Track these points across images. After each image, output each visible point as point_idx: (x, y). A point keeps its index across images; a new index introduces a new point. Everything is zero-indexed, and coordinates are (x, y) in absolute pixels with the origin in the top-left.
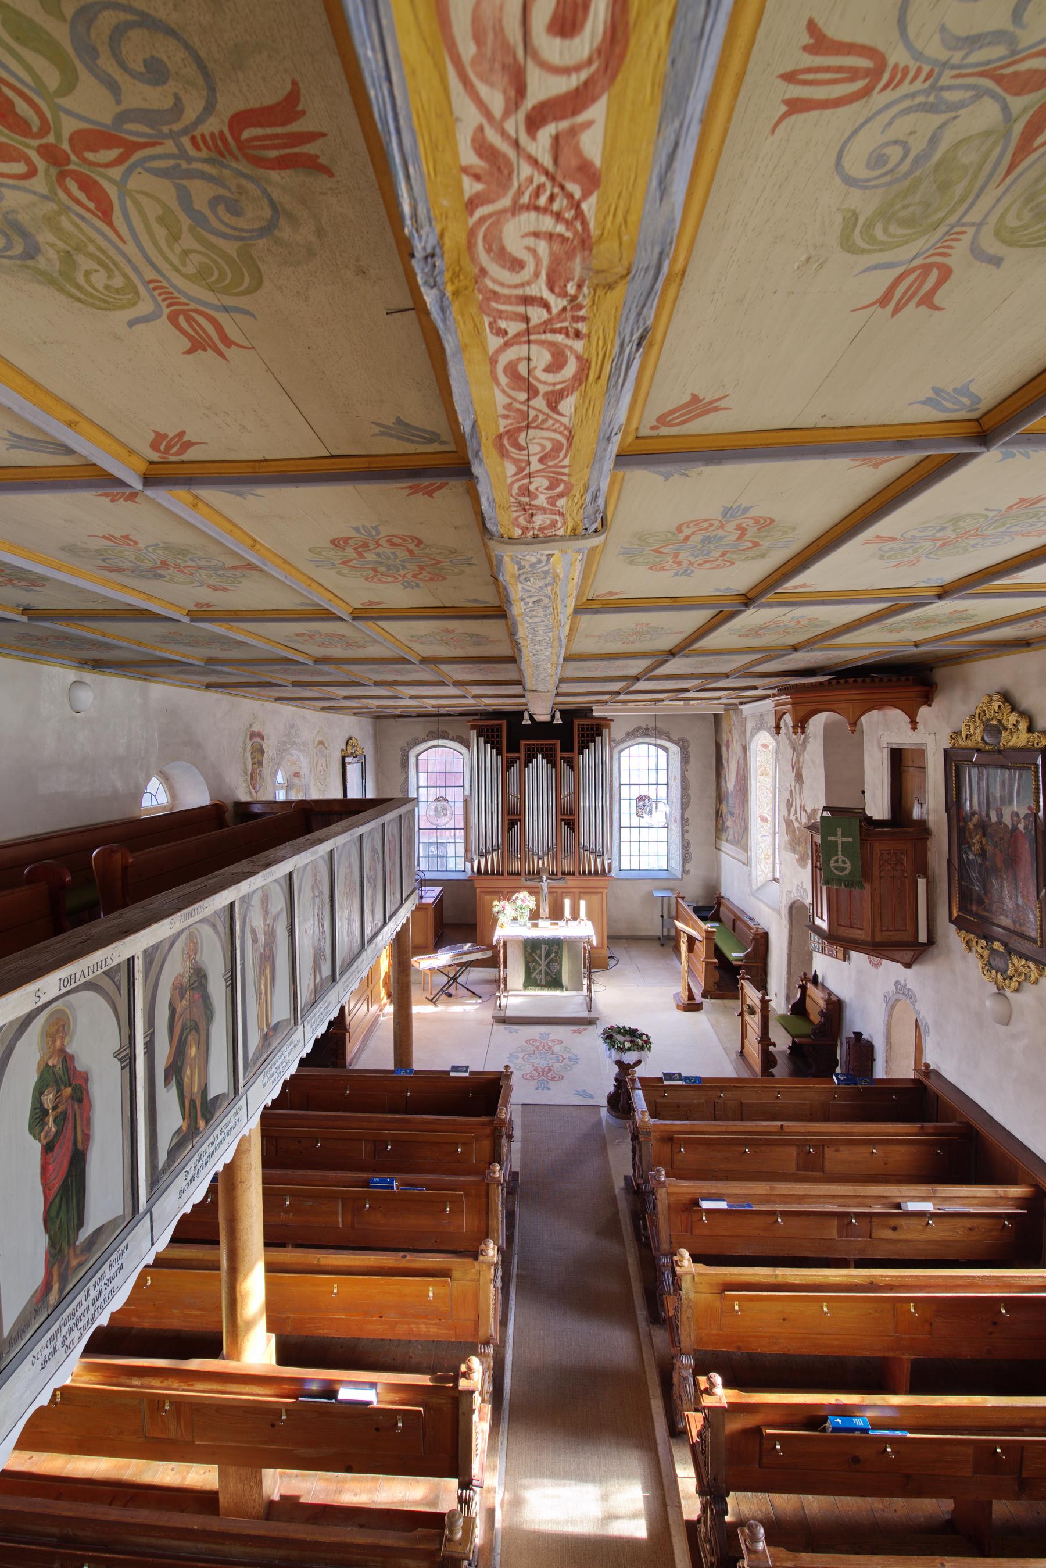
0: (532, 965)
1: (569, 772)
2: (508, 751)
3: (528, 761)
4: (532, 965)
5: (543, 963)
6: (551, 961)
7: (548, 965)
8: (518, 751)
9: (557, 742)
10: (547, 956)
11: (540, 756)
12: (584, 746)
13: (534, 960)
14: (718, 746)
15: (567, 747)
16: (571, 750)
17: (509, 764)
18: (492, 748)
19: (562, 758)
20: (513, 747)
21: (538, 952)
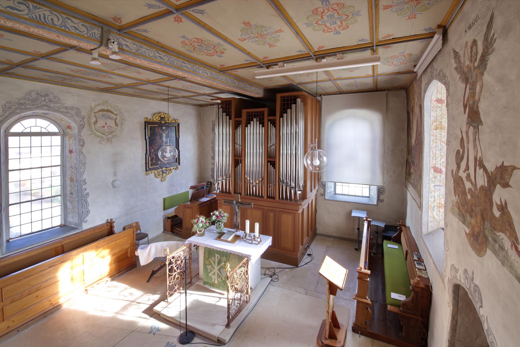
0: (209, 267)
1: (274, 130)
2: (236, 117)
3: (248, 123)
4: (209, 267)
5: (217, 268)
6: (222, 267)
7: (219, 270)
8: (241, 117)
9: (266, 110)
10: (219, 263)
11: (255, 119)
12: (284, 111)
13: (211, 264)
14: (408, 113)
15: (272, 113)
16: (275, 115)
17: (236, 125)
18: (227, 115)
19: (269, 120)
20: (239, 115)
21: (213, 258)
